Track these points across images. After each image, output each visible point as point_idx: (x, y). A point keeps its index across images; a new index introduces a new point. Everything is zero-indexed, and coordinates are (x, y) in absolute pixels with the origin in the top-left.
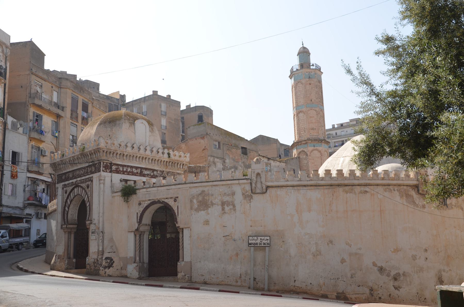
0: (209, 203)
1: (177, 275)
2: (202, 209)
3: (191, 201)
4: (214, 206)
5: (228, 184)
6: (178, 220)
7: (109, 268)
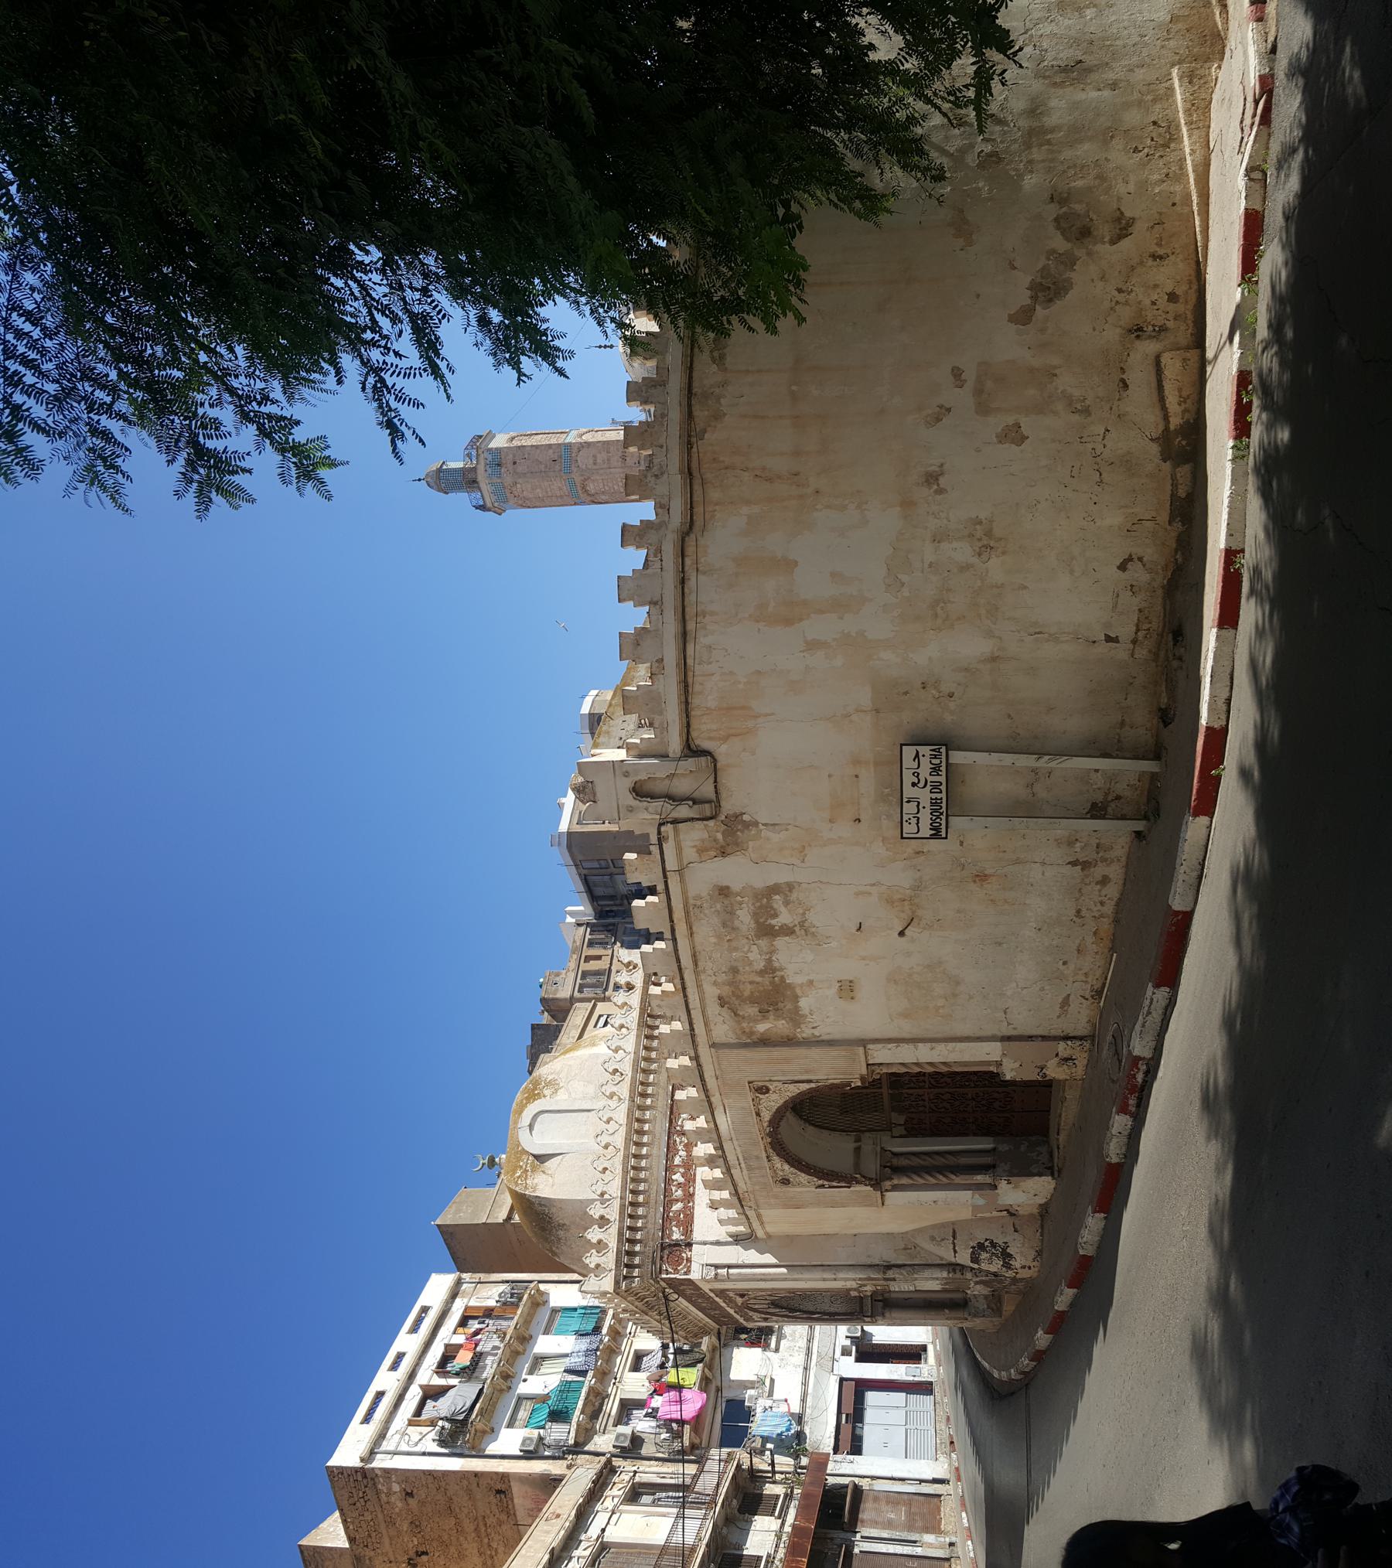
2: (789, 1006)
3: (765, 1042)
4: (776, 964)
5: (687, 913)
7: (1010, 1256)
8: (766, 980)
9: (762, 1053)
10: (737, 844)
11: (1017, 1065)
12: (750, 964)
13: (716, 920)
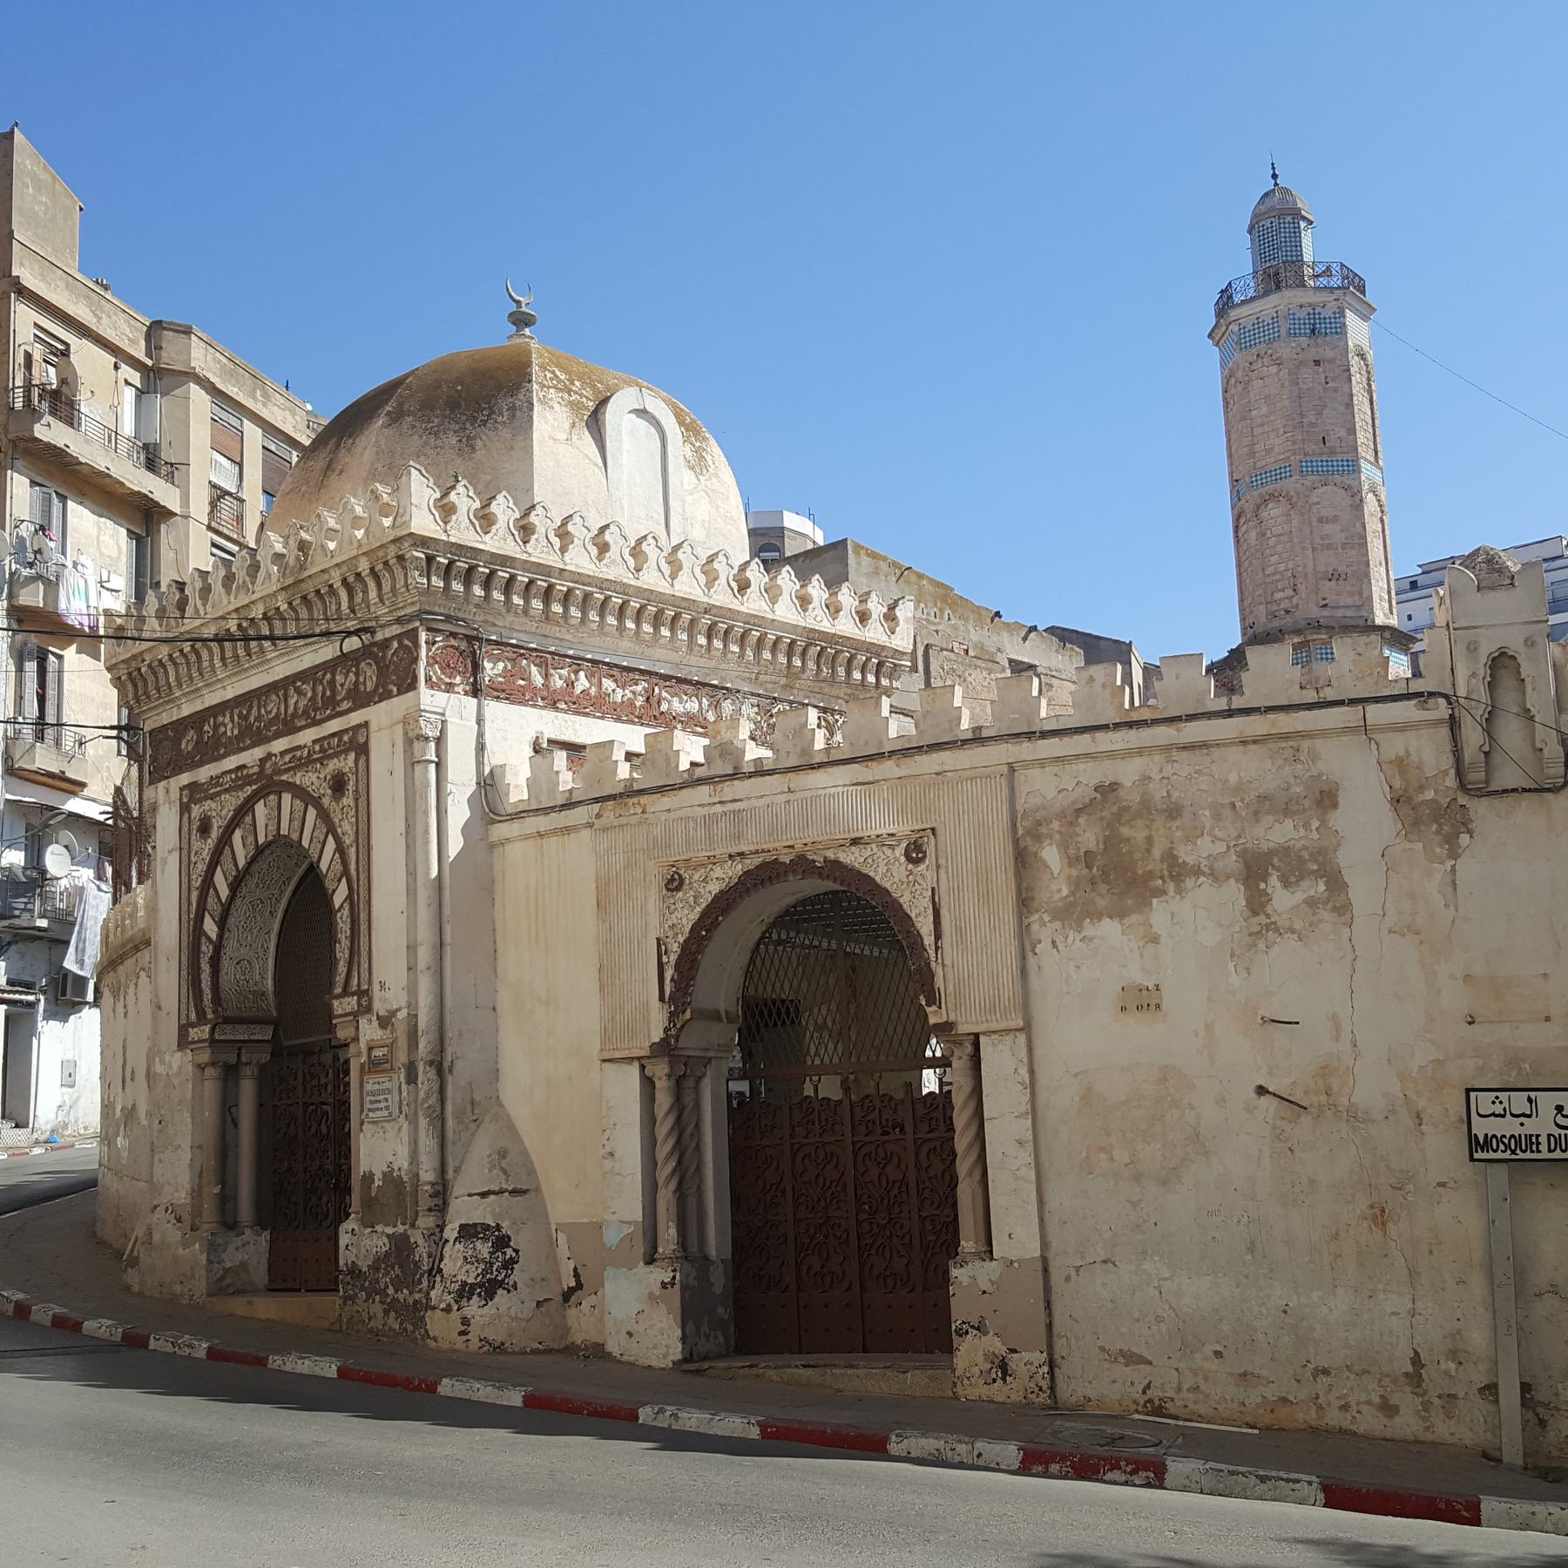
1: (949, 1350)
2: (1101, 903)
3: (1023, 860)
4: (1189, 883)
5: (1285, 737)
6: (939, 982)
8: (1155, 862)
10: (1416, 823)
11: (986, 1286)
12: (1189, 839)
13: (1271, 784)
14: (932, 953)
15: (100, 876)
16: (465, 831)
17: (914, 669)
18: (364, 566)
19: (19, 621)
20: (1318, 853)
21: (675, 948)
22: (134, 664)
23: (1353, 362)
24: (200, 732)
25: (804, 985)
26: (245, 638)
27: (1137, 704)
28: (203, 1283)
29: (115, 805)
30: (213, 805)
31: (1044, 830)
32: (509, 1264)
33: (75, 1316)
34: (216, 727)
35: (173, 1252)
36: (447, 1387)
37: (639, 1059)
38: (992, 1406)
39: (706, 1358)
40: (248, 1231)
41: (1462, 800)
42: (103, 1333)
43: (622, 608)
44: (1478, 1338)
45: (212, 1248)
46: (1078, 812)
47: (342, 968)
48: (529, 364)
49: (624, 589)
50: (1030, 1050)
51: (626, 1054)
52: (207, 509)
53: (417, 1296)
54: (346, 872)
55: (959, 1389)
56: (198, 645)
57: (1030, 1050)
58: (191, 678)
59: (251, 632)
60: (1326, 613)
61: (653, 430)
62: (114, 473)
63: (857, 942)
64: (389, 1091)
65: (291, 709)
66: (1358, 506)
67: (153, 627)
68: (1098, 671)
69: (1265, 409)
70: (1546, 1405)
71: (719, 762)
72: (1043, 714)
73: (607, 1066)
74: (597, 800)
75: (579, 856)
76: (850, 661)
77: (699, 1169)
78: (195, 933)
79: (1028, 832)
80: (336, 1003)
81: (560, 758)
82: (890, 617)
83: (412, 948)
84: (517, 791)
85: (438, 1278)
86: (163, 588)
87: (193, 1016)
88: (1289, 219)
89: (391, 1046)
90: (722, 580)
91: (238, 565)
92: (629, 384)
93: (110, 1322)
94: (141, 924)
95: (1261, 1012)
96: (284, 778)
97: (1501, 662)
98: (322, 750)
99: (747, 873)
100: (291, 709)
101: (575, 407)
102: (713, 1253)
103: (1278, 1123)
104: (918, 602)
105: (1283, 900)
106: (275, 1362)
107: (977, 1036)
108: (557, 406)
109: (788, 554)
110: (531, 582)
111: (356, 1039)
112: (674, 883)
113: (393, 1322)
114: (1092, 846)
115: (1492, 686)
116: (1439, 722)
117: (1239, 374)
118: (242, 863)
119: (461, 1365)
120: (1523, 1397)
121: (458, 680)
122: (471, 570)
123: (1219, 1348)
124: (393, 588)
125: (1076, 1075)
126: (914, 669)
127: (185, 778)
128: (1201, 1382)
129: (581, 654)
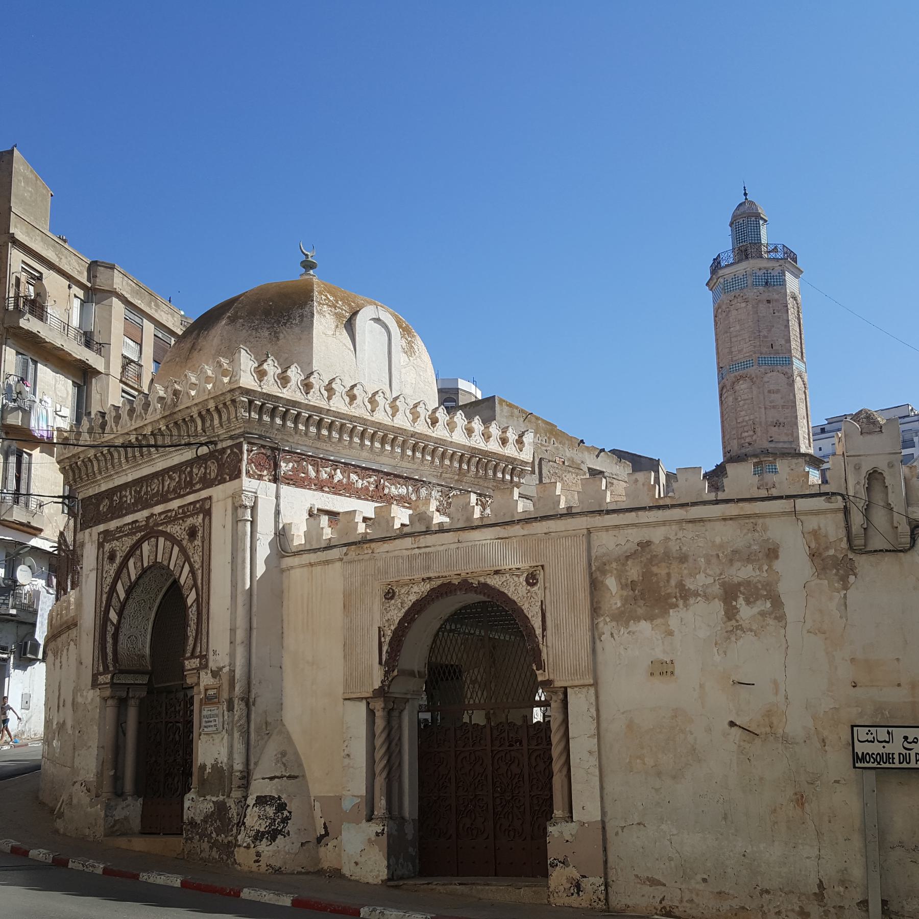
0: (672, 588)
1: (546, 875)
2: (640, 611)
3: (595, 585)
4: (692, 601)
5: (748, 516)
6: (544, 656)
8: (672, 588)
9: (581, 581)
10: (824, 569)
12: (692, 575)
14: (540, 639)
15: (49, 584)
16: (267, 561)
17: (533, 472)
18: (211, 405)
19: (7, 433)
20: (767, 584)
21: (389, 633)
22: (73, 460)
23: (789, 302)
24: (112, 501)
25: (465, 656)
26: (140, 446)
27: (662, 495)
28: (102, 829)
29: (59, 542)
30: (118, 544)
31: (607, 567)
32: (285, 820)
33: (26, 847)
34: (121, 498)
35: (84, 809)
36: (246, 894)
37: (366, 698)
38: (571, 910)
39: (401, 878)
40: (129, 798)
41: (851, 556)
42: (41, 857)
43: (363, 433)
44: (857, 873)
45: (108, 808)
46: (627, 557)
47: (191, 641)
48: (312, 291)
49: (364, 421)
50: (597, 697)
51: (358, 695)
52: (120, 370)
53: (230, 838)
54: (195, 585)
55: (552, 899)
56: (112, 449)
57: (597, 697)
58: (107, 469)
59: (144, 442)
60: (772, 445)
61: (383, 330)
62: (66, 348)
63: (497, 632)
64: (217, 716)
65: (166, 488)
66: (791, 384)
67: (85, 438)
68: (640, 476)
69: (738, 328)
70: (896, 914)
71: (418, 524)
72: (608, 500)
73: (347, 702)
74: (345, 545)
75: (334, 578)
76: (496, 466)
77: (400, 765)
78: (104, 620)
79: (598, 569)
80: (186, 662)
81: (324, 520)
82: (520, 442)
83: (233, 631)
84: (298, 538)
85: (243, 828)
86: (93, 416)
87: (101, 669)
88: (753, 219)
89: (219, 688)
90: (422, 417)
91: (138, 402)
92: (370, 303)
93: (45, 851)
94: (72, 613)
95: (733, 678)
96: (160, 528)
97: (874, 476)
98: (184, 512)
99: (432, 590)
100: (166, 488)
101: (338, 316)
102: (407, 815)
103: (742, 743)
104: (536, 433)
105: (746, 612)
106: (144, 877)
107: (566, 688)
108: (327, 315)
109: (460, 404)
110: (310, 416)
111: (198, 684)
112: (390, 595)
113: (215, 854)
114: (635, 579)
115: (868, 489)
116: (836, 511)
117: (724, 307)
118: (133, 578)
119: (255, 881)
120: (883, 907)
121: (265, 473)
122: (275, 408)
123: (705, 877)
124: (229, 419)
125: (623, 713)
126: (533, 472)
127: (102, 528)
128: (694, 897)
129: (338, 459)
